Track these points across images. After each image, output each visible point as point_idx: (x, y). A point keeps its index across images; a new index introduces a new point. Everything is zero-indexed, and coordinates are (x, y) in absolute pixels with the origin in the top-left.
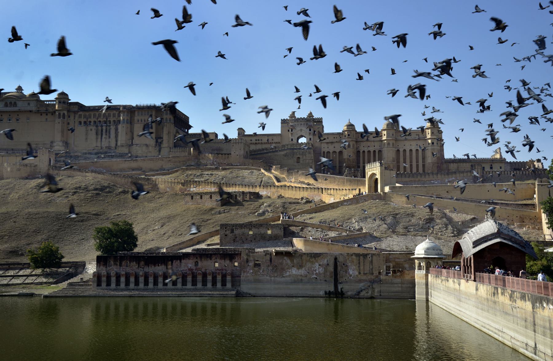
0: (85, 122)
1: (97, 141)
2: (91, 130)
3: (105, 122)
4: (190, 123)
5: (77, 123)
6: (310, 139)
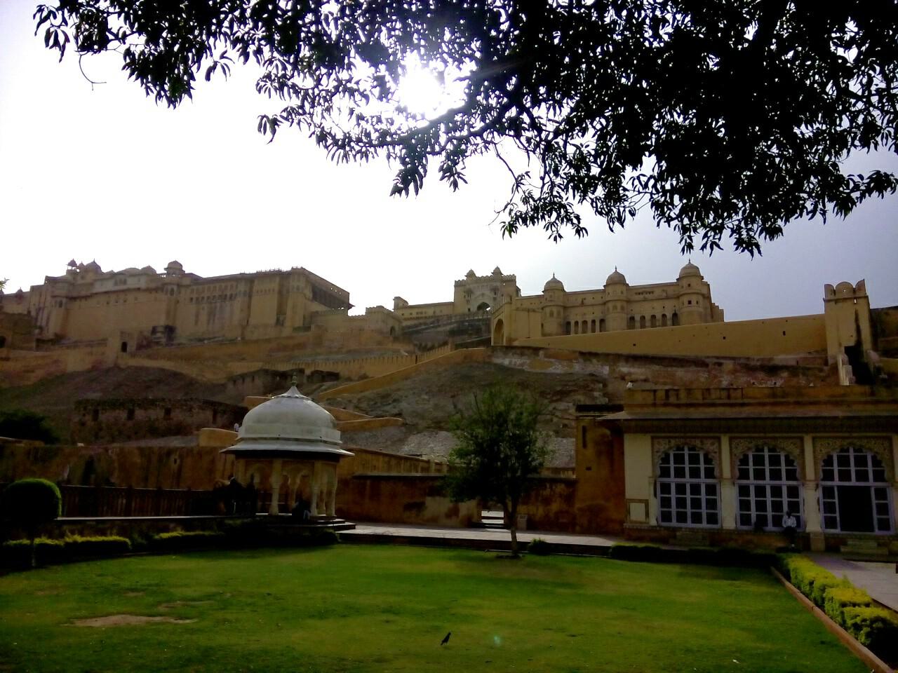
0: (197, 299)
1: (208, 323)
2: (203, 309)
4: (351, 302)
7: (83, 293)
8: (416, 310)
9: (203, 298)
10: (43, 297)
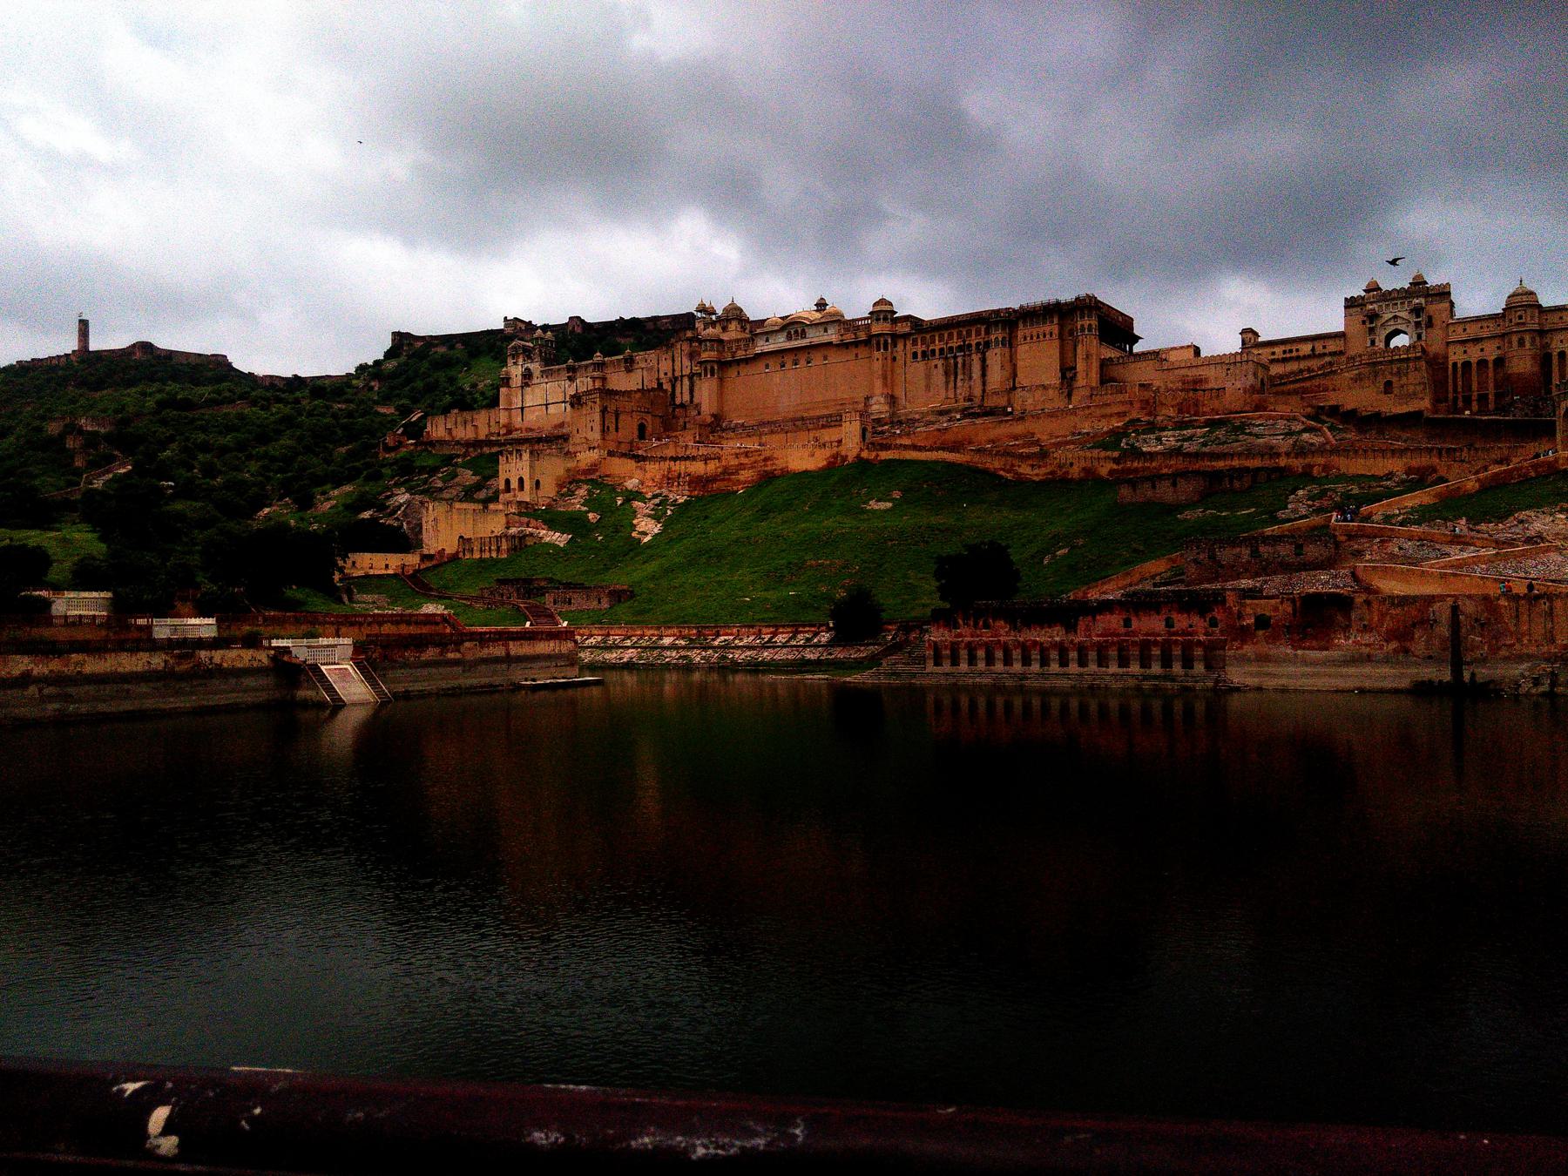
3: (960, 348)
4: (1136, 332)
5: (909, 356)
6: (1419, 337)
7: (740, 354)
8: (1283, 348)
9: (933, 352)
10: (678, 364)
